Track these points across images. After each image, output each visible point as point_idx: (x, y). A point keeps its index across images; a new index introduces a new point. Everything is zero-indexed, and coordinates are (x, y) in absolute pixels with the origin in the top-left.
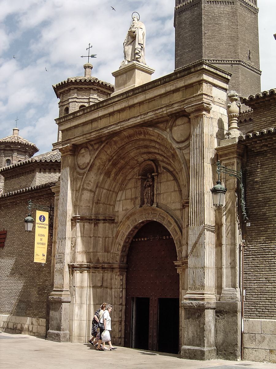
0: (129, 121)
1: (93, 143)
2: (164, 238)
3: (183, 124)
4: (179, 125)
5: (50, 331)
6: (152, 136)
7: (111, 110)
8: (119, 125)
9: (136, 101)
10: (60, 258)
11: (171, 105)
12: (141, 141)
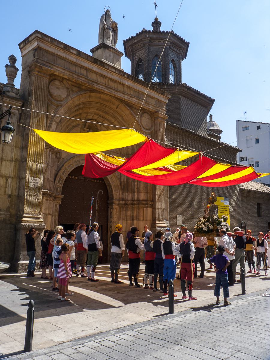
0: (118, 93)
1: (70, 83)
2: (93, 181)
5: (28, 262)
7: (105, 73)
8: (109, 89)
9: (109, 75)
10: (34, 183)
12: (107, 107)
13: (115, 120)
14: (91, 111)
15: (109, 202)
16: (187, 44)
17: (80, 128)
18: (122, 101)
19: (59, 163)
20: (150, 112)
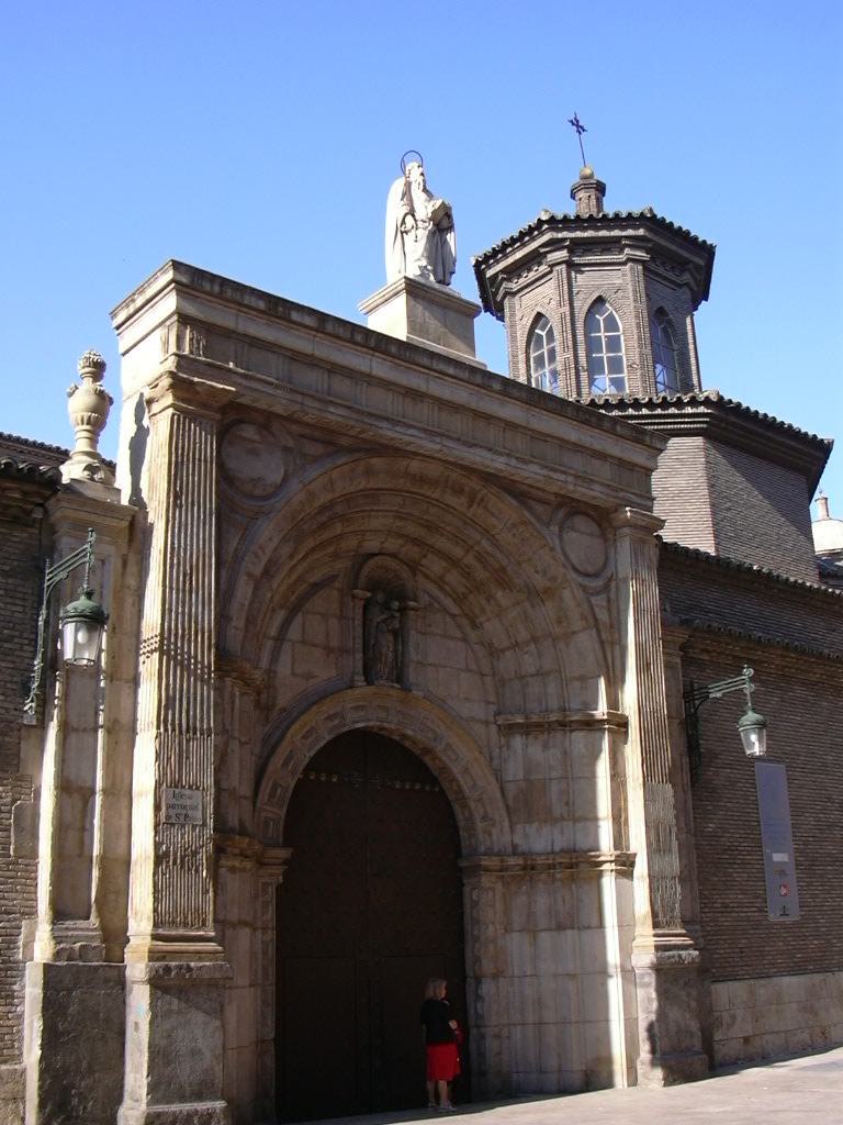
2: (398, 786)
3: (588, 534)
4: (582, 533)
6: (492, 514)
8: (438, 440)
11: (586, 479)
12: (434, 505)
13: (467, 551)
14: (375, 523)
15: (463, 864)
16: (707, 252)
17: (338, 590)
18: (489, 478)
19: (266, 729)
20: (596, 507)
